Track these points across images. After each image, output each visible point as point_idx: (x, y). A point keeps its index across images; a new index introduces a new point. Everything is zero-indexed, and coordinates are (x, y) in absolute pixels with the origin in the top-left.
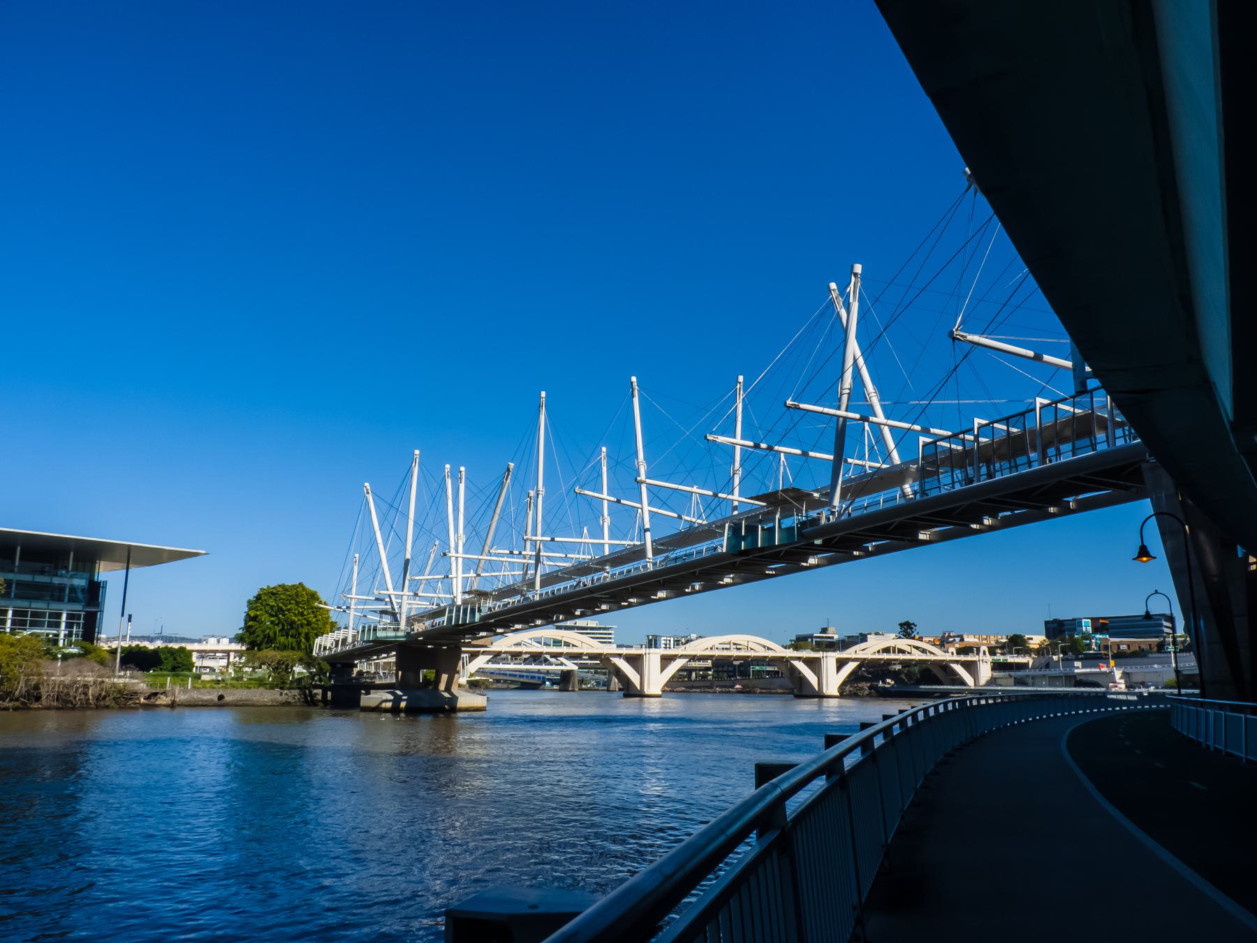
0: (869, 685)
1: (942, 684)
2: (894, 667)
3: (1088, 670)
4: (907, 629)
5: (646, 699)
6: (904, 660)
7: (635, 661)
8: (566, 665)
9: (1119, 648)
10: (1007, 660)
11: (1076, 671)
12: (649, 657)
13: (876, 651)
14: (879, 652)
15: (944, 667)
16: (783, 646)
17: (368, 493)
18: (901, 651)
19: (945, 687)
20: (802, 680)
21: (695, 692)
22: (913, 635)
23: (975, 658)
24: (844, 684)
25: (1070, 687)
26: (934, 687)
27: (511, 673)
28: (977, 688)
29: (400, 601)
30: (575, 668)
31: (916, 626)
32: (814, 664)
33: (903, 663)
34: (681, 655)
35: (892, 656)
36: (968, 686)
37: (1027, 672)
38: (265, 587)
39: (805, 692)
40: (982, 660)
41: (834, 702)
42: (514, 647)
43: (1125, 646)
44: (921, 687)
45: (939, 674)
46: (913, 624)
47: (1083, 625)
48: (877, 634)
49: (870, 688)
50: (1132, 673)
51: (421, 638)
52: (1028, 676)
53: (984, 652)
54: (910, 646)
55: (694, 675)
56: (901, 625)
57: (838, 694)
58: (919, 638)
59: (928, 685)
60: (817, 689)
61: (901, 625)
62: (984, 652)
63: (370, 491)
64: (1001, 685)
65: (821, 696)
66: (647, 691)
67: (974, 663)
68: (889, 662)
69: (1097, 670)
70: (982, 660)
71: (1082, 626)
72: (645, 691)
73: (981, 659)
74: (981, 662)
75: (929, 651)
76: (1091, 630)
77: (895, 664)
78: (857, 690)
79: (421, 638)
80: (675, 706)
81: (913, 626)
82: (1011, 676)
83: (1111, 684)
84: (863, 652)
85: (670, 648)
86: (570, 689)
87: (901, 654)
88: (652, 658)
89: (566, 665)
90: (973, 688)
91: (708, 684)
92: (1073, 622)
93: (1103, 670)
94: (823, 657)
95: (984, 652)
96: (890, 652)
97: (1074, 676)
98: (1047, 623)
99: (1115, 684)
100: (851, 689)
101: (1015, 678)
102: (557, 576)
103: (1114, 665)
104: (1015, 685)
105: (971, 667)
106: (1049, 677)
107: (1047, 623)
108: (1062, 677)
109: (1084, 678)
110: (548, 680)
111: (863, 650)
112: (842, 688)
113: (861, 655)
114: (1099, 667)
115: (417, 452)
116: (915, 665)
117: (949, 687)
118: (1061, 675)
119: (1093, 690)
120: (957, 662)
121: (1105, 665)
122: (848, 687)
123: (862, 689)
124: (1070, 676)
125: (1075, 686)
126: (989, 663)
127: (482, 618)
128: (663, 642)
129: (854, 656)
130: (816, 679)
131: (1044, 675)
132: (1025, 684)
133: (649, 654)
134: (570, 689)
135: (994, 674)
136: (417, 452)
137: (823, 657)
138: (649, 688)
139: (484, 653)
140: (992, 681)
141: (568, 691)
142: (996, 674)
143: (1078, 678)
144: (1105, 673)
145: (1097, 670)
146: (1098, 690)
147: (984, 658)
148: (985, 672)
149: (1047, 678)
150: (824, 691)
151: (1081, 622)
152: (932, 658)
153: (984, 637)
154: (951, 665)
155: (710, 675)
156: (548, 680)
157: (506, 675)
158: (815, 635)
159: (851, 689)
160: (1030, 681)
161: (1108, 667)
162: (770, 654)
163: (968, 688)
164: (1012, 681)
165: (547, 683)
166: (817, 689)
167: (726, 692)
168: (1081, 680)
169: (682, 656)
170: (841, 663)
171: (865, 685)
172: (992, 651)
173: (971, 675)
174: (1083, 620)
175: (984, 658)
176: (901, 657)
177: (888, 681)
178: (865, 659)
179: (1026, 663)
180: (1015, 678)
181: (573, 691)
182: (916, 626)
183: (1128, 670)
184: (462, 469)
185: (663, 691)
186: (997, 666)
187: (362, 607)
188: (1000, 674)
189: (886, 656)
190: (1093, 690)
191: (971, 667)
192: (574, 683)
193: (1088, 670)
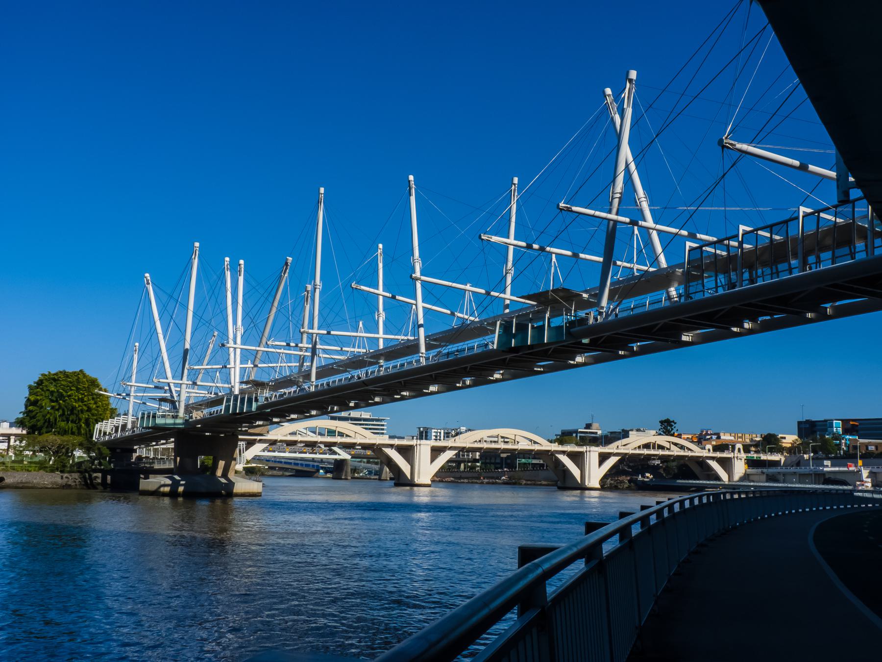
0: (629, 478)
1: (698, 479)
2: (653, 462)
3: (837, 469)
4: (667, 427)
5: (415, 488)
6: (663, 455)
7: (407, 452)
8: (339, 455)
9: (867, 448)
10: (760, 457)
11: (825, 469)
15: (701, 462)
16: (548, 440)
17: (148, 283)
18: (661, 447)
19: (701, 482)
20: (566, 472)
21: (463, 482)
22: (672, 432)
23: (731, 455)
24: (605, 477)
25: (819, 484)
26: (690, 481)
27: (286, 461)
28: (730, 483)
29: (179, 389)
30: (348, 457)
31: (675, 423)
32: (578, 458)
33: (661, 458)
34: (451, 447)
35: (652, 452)
36: (723, 481)
37: (778, 470)
38: (47, 373)
39: (568, 485)
40: (737, 457)
42: (289, 436)
43: (873, 447)
44: (678, 481)
45: (696, 469)
46: (673, 422)
47: (834, 426)
48: (638, 430)
50: (879, 473)
51: (200, 426)
52: (779, 473)
54: (669, 442)
55: (462, 466)
56: (661, 422)
57: (598, 486)
58: (679, 435)
59: (684, 479)
60: (579, 482)
61: (661, 422)
62: (739, 450)
63: (150, 282)
64: (753, 481)
65: (583, 488)
66: (417, 481)
68: (649, 457)
69: (846, 469)
70: (737, 457)
71: (832, 427)
72: (416, 480)
73: (736, 455)
75: (687, 448)
76: (841, 431)
77: (654, 459)
78: (617, 483)
79: (200, 426)
80: (444, 495)
81: (673, 424)
82: (763, 473)
83: (858, 483)
84: (624, 447)
85: (440, 440)
87: (660, 450)
88: (424, 449)
89: (339, 455)
90: (727, 483)
91: (476, 475)
92: (824, 423)
93: (851, 469)
95: (739, 450)
96: (650, 448)
97: (824, 474)
98: (800, 423)
99: (862, 483)
100: (612, 482)
101: (767, 475)
102: (333, 368)
103: (861, 465)
104: (767, 481)
105: (726, 464)
107: (800, 423)
108: (812, 474)
109: (832, 476)
110: (322, 468)
111: (624, 445)
112: (603, 481)
113: (622, 450)
114: (848, 466)
115: (197, 244)
116: (673, 461)
117: (705, 482)
118: (811, 473)
119: (841, 487)
120: (713, 458)
121: (853, 465)
123: (622, 482)
124: (819, 474)
125: (823, 484)
126: (743, 460)
127: (258, 408)
128: (434, 434)
129: (616, 451)
131: (795, 473)
132: (777, 481)
133: (420, 445)
134: (343, 477)
136: (197, 244)
138: (419, 477)
139: (260, 441)
140: (746, 477)
141: (341, 479)
142: (750, 471)
143: (827, 476)
144: (853, 472)
145: (846, 469)
146: (845, 487)
147: (739, 455)
148: (740, 468)
150: (586, 484)
151: (833, 423)
152: (690, 454)
153: (740, 435)
154: (707, 461)
155: (478, 466)
156: (322, 468)
157: (281, 462)
158: (579, 430)
159: (612, 482)
160: (781, 478)
161: (856, 466)
162: (536, 447)
163: (722, 483)
164: (764, 477)
165: (321, 471)
166: (579, 482)
167: (493, 483)
168: (829, 478)
169: (451, 448)
170: (603, 458)
171: (625, 479)
172: (747, 449)
173: (726, 472)
174: (834, 421)
175: (739, 455)
176: (661, 452)
177: (648, 475)
178: (626, 454)
180: (767, 475)
181: (346, 479)
182: (675, 423)
183: (875, 470)
184: (242, 262)
185: (433, 481)
186: (751, 463)
187: (142, 394)
189: (646, 452)
190: (841, 487)
191: (726, 464)
192: (346, 472)
193: (837, 469)
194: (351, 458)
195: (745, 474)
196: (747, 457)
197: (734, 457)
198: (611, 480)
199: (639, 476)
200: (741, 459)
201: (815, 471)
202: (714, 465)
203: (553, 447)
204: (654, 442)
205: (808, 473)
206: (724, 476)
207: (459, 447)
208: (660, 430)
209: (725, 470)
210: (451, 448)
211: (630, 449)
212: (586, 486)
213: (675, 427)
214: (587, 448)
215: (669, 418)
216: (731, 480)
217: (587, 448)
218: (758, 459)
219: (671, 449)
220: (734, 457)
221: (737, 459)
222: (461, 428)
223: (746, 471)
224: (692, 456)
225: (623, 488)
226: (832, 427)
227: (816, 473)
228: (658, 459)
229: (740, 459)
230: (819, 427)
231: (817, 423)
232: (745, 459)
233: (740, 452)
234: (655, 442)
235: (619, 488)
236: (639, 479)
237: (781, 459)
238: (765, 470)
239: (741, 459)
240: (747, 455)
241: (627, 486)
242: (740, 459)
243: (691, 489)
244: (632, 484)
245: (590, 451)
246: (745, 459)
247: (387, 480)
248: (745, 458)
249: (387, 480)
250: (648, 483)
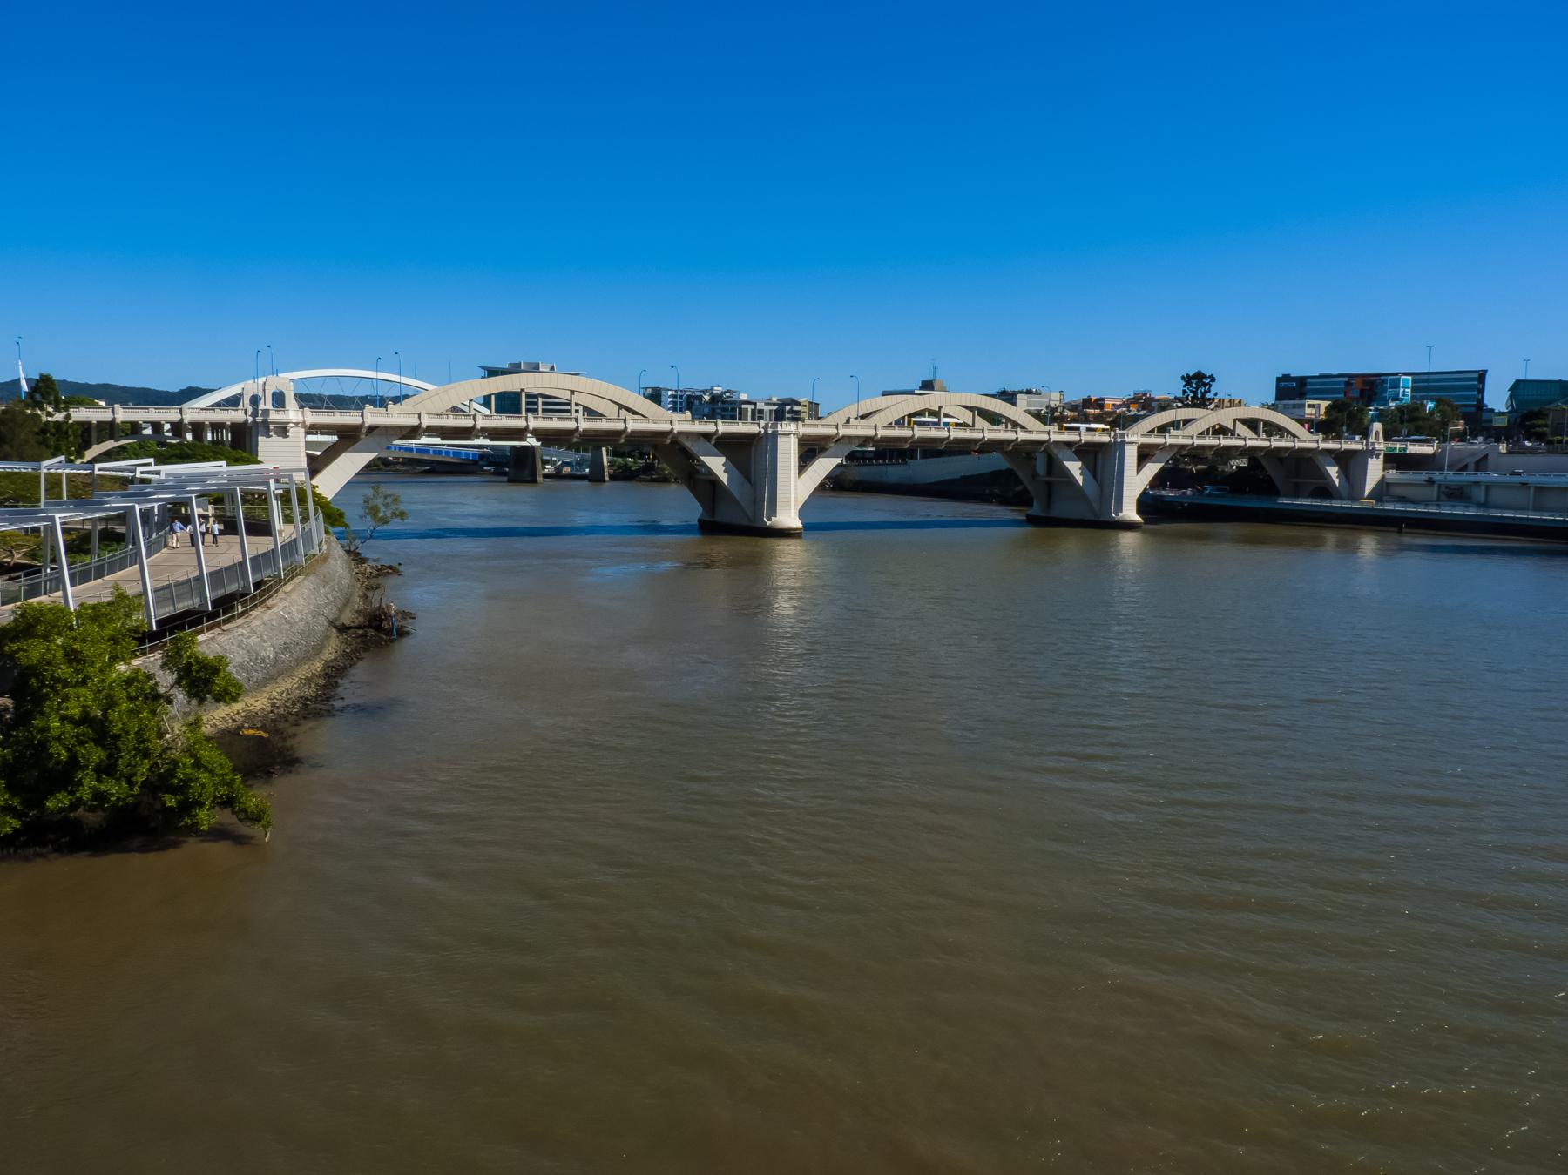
10: (1405, 449)
13: (1205, 428)
14: (1152, 432)
52: (1477, 484)
53: (1377, 433)
56: (1188, 380)
61: (1183, 378)
62: (1377, 433)
68: (1226, 453)
71: (1398, 387)
82: (1430, 482)
101: (1440, 486)
105: (1351, 463)
113: (1175, 438)
126: (1382, 456)
142: (1393, 474)
149: (1532, 491)
151: (1399, 379)
160: (1479, 494)
178: (1183, 447)
182: (1213, 379)
186: (1392, 460)
189: (1210, 441)
207: (858, 437)
218: (1402, 452)
219: (1237, 431)
222: (715, 388)
226: (1398, 387)
230: (1309, 387)
231: (1309, 380)
232: (1385, 455)
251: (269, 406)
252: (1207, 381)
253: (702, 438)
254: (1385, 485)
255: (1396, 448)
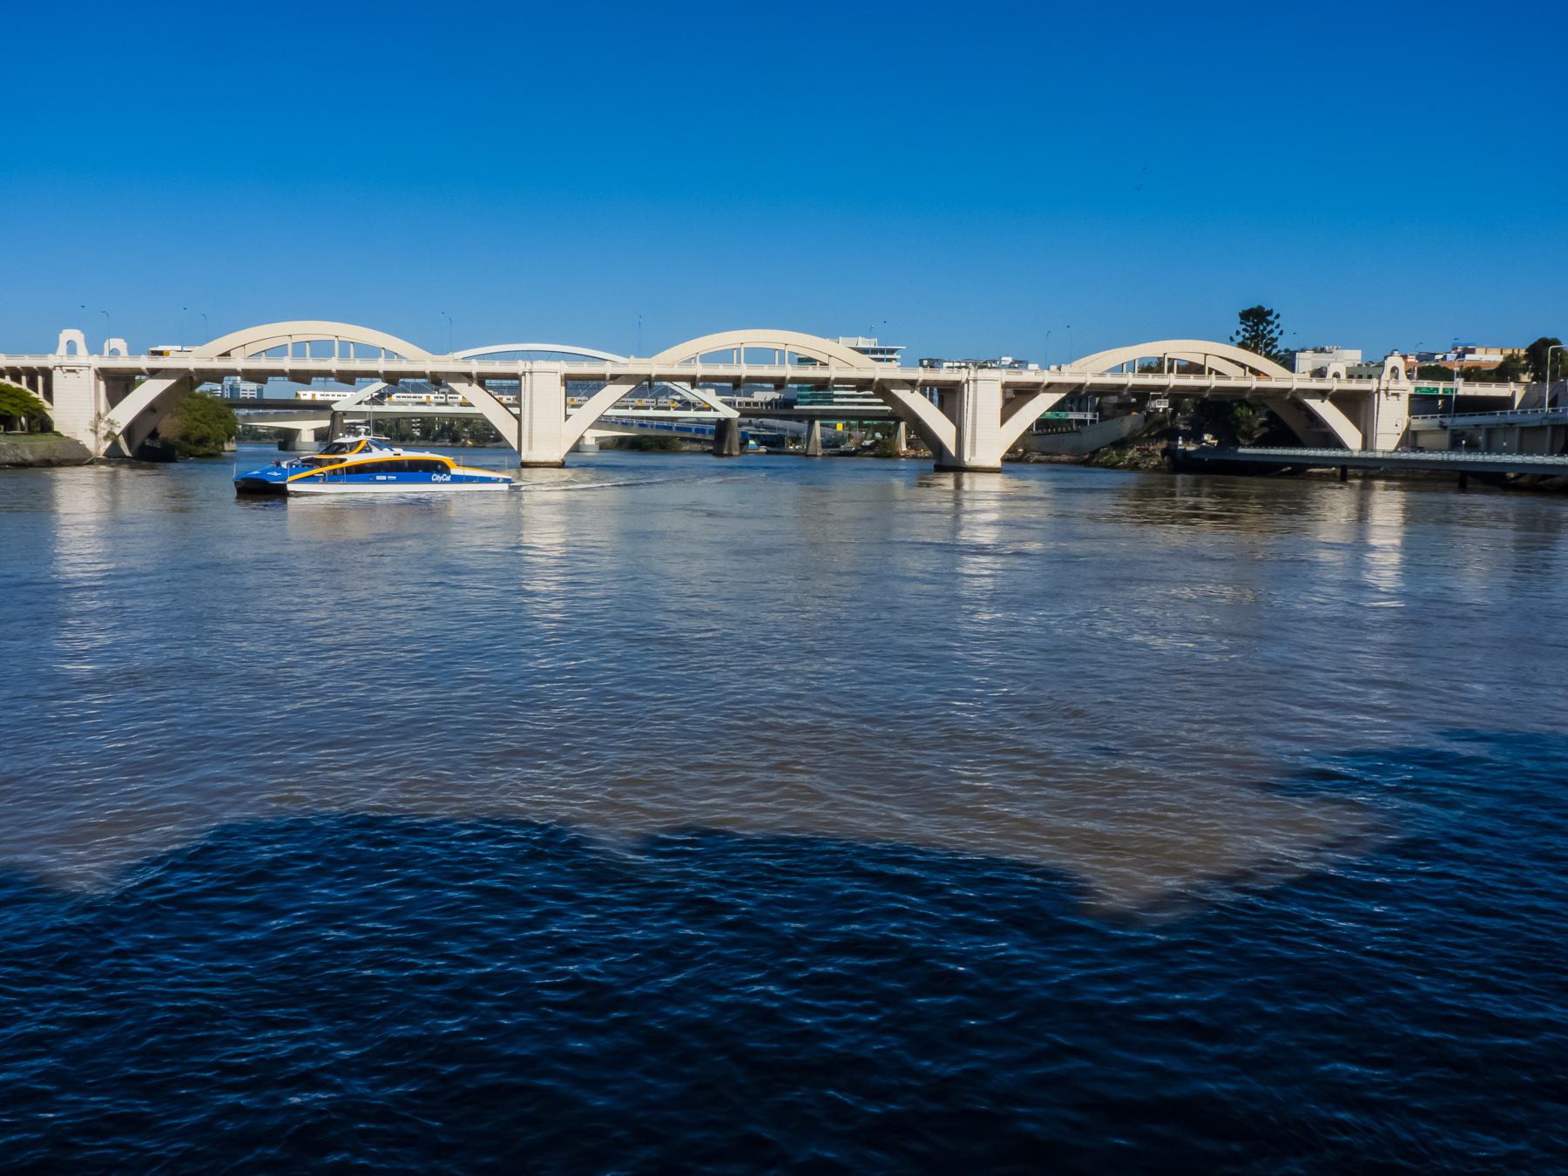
1: (1302, 445)
8: (715, 410)
12: (532, 380)
19: (1306, 452)
23: (1371, 385)
25: (1551, 453)
27: (660, 423)
28: (1370, 455)
30: (733, 414)
33: (1177, 395)
35: (1151, 380)
36: (1349, 450)
39: (946, 462)
40: (1387, 391)
41: (995, 483)
44: (1241, 450)
46: (1270, 313)
49: (1165, 452)
56: (1246, 316)
57: (997, 463)
60: (952, 450)
61: (1246, 316)
62: (1394, 369)
67: (1366, 396)
68: (1143, 393)
70: (1387, 391)
73: (1383, 386)
74: (1383, 394)
75: (1250, 367)
82: (1443, 427)
86: (725, 452)
89: (715, 410)
90: (1356, 454)
94: (968, 381)
105: (1356, 405)
106: (1523, 429)
108: (1544, 428)
110: (753, 437)
118: (1545, 423)
122: (1130, 453)
123: (1151, 455)
126: (1405, 399)
130: (953, 429)
132: (1473, 447)
133: (531, 373)
134: (725, 452)
135: (1415, 422)
137: (968, 381)
140: (1410, 439)
142: (1418, 423)
147: (1392, 385)
149: (1517, 432)
150: (966, 459)
156: (753, 437)
157: (689, 430)
163: (1347, 454)
164: (1445, 438)
165: (752, 442)
166: (954, 455)
170: (1016, 396)
173: (1359, 430)
176: (1172, 380)
177: (1207, 437)
178: (1081, 386)
179: (1508, 398)
180: (1453, 431)
181: (730, 455)
182: (1277, 317)
185: (1005, 460)
188: (1426, 422)
192: (730, 443)
194: (740, 416)
195: (1407, 429)
196: (1417, 389)
197: (1378, 391)
198: (1138, 450)
199: (1177, 440)
200: (1397, 395)
201: (1554, 419)
202: (1328, 412)
203: (878, 370)
204: (1162, 356)
205: (1537, 424)
206: (1351, 436)
208: (1238, 333)
209: (1356, 422)
210: (615, 378)
211: (1089, 374)
212: (964, 462)
213: (1278, 326)
214: (969, 373)
215: (1264, 306)
216: (1369, 447)
217: (969, 373)
220: (1378, 391)
221: (1387, 394)
223: (1409, 424)
224: (1258, 390)
225: (1146, 467)
227: (1555, 423)
228: (1164, 398)
229: (1393, 394)
232: (1411, 396)
233: (1397, 377)
234: (1165, 354)
235: (1139, 468)
236: (1179, 448)
237: (1514, 393)
238: (1448, 421)
239: (1397, 395)
240: (1419, 385)
241: (1156, 463)
242: (1393, 394)
243: (1284, 470)
244: (1166, 458)
245: (975, 381)
246: (1411, 396)
247: (816, 456)
248: (1412, 392)
249: (816, 456)
250: (1200, 456)
251: (65, 353)
252: (1270, 318)
253: (464, 378)
254: (1410, 433)
255: (1437, 389)
